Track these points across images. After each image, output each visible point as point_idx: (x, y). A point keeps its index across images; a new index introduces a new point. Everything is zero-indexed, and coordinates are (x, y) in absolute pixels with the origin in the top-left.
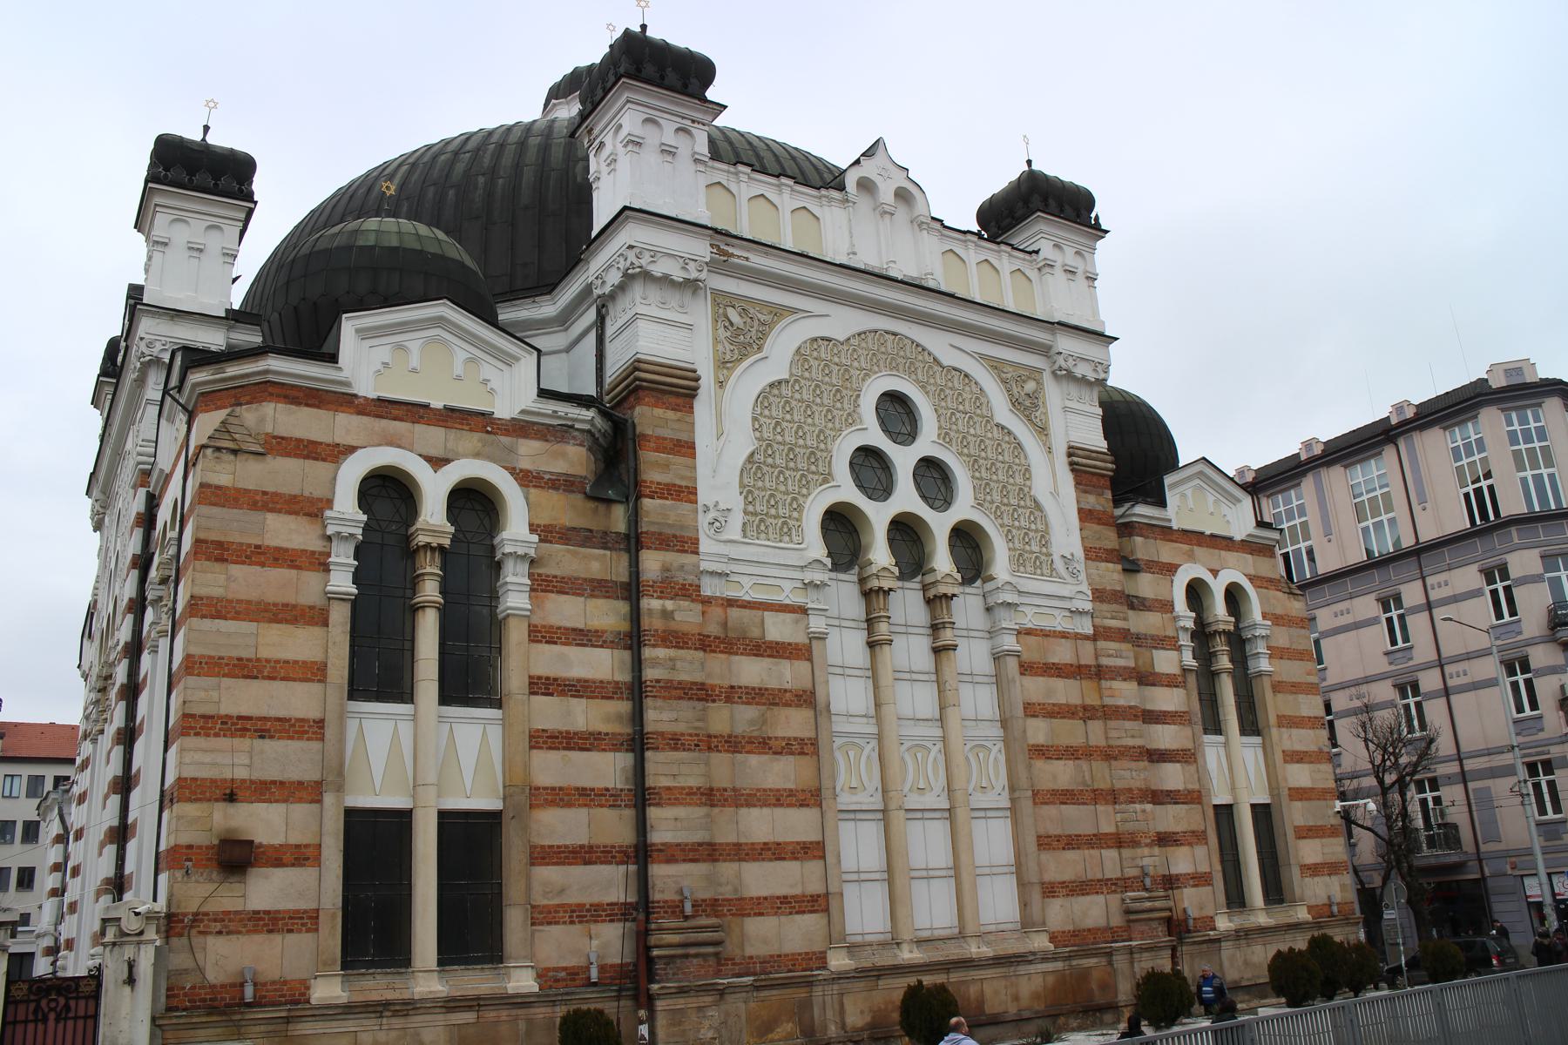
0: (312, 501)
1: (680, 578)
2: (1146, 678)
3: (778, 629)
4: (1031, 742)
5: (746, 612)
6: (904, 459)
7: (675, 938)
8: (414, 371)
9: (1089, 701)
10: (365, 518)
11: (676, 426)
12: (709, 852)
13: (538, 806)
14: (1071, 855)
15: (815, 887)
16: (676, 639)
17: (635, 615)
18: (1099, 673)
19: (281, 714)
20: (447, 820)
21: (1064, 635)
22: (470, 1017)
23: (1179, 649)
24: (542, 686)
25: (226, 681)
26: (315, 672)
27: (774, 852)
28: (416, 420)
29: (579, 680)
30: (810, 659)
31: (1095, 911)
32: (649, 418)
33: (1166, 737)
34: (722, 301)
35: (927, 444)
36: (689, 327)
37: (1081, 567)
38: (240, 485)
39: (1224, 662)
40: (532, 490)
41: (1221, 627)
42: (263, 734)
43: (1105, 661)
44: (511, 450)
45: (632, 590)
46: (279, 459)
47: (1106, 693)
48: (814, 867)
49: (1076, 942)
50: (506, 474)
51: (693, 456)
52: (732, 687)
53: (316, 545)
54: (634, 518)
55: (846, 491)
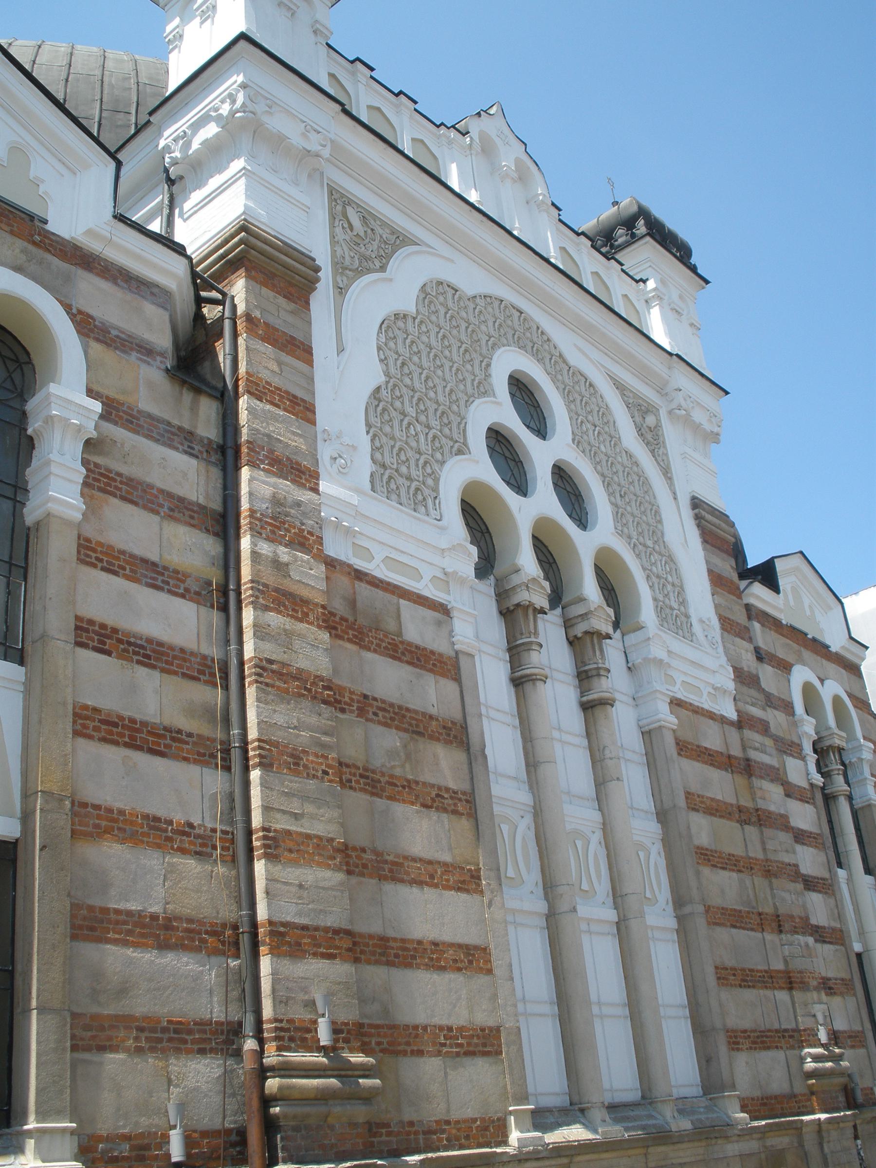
4: (697, 842)
5: (381, 593)
6: (541, 455)
9: (742, 803)
11: (290, 319)
13: (86, 835)
14: (749, 995)
17: (229, 560)
18: (747, 768)
23: (803, 758)
24: (96, 636)
29: (149, 641)
30: (457, 679)
33: (809, 860)
37: (718, 638)
41: (837, 742)
43: (753, 755)
47: (759, 794)
52: (365, 697)
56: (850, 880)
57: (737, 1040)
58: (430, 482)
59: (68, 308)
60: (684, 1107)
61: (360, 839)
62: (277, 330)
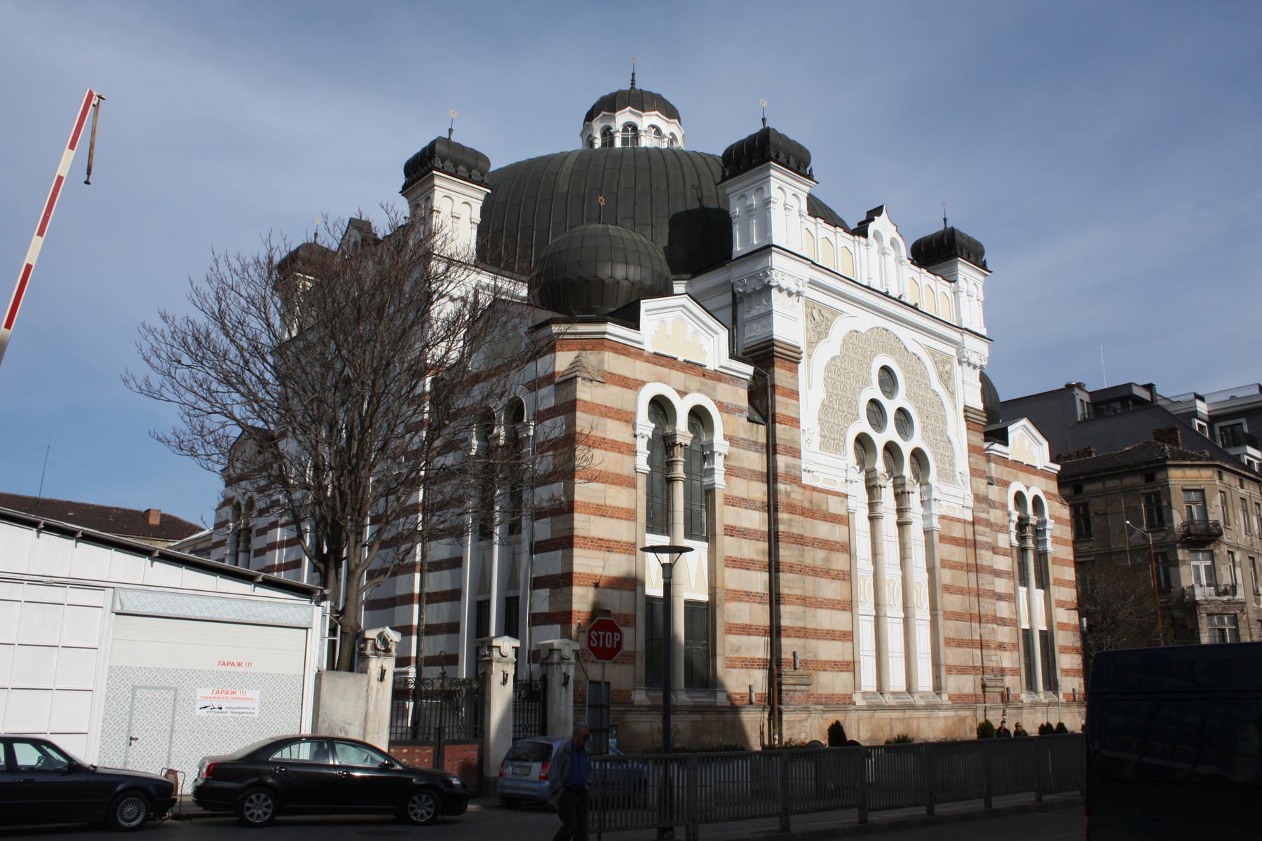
0: (627, 413)
1: (793, 472)
2: (995, 550)
3: (834, 506)
6: (890, 407)
7: (792, 681)
10: (653, 425)
12: (803, 633)
14: (960, 650)
15: (849, 658)
16: (792, 509)
19: (617, 539)
20: (691, 606)
21: (959, 520)
22: (698, 717)
24: (731, 531)
25: (593, 518)
26: (630, 515)
27: (831, 635)
31: (967, 684)
32: (780, 375)
33: (1002, 585)
34: (811, 304)
36: (795, 319)
39: (1030, 543)
42: (609, 550)
44: (714, 389)
45: (771, 477)
48: (849, 644)
49: (960, 701)
53: (630, 440)
54: (771, 434)
55: (863, 426)
56: (1028, 593)
57: (950, 670)
60: (924, 695)
61: (809, 594)
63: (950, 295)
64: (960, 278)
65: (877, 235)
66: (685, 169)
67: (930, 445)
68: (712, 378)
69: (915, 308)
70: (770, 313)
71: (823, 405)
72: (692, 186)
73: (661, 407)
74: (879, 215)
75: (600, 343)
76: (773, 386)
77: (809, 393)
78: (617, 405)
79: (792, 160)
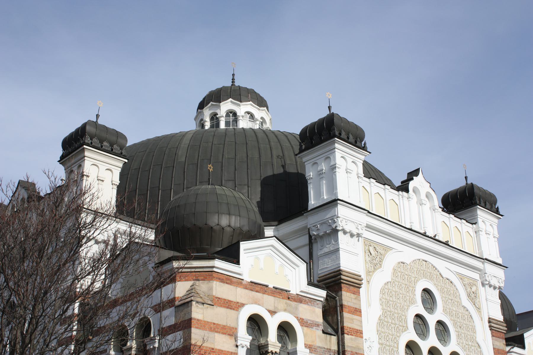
0: (231, 328)
6: (432, 320)
8: (262, 269)
10: (251, 338)
11: (354, 301)
28: (264, 292)
34: (368, 242)
35: (439, 314)
36: (357, 255)
38: (206, 320)
40: (305, 328)
44: (297, 308)
46: (218, 308)
50: (296, 319)
51: (361, 316)
53: (233, 349)
55: (411, 335)
58: (396, 345)
59: (297, 318)
62: (351, 307)
63: (472, 233)
64: (480, 221)
65: (415, 190)
66: (272, 143)
67: (463, 348)
68: (295, 300)
69: (446, 244)
70: (337, 250)
71: (380, 319)
72: (278, 157)
73: (256, 323)
74: (417, 175)
75: (209, 275)
76: (342, 306)
77: (369, 311)
78: (223, 323)
79: (351, 137)
